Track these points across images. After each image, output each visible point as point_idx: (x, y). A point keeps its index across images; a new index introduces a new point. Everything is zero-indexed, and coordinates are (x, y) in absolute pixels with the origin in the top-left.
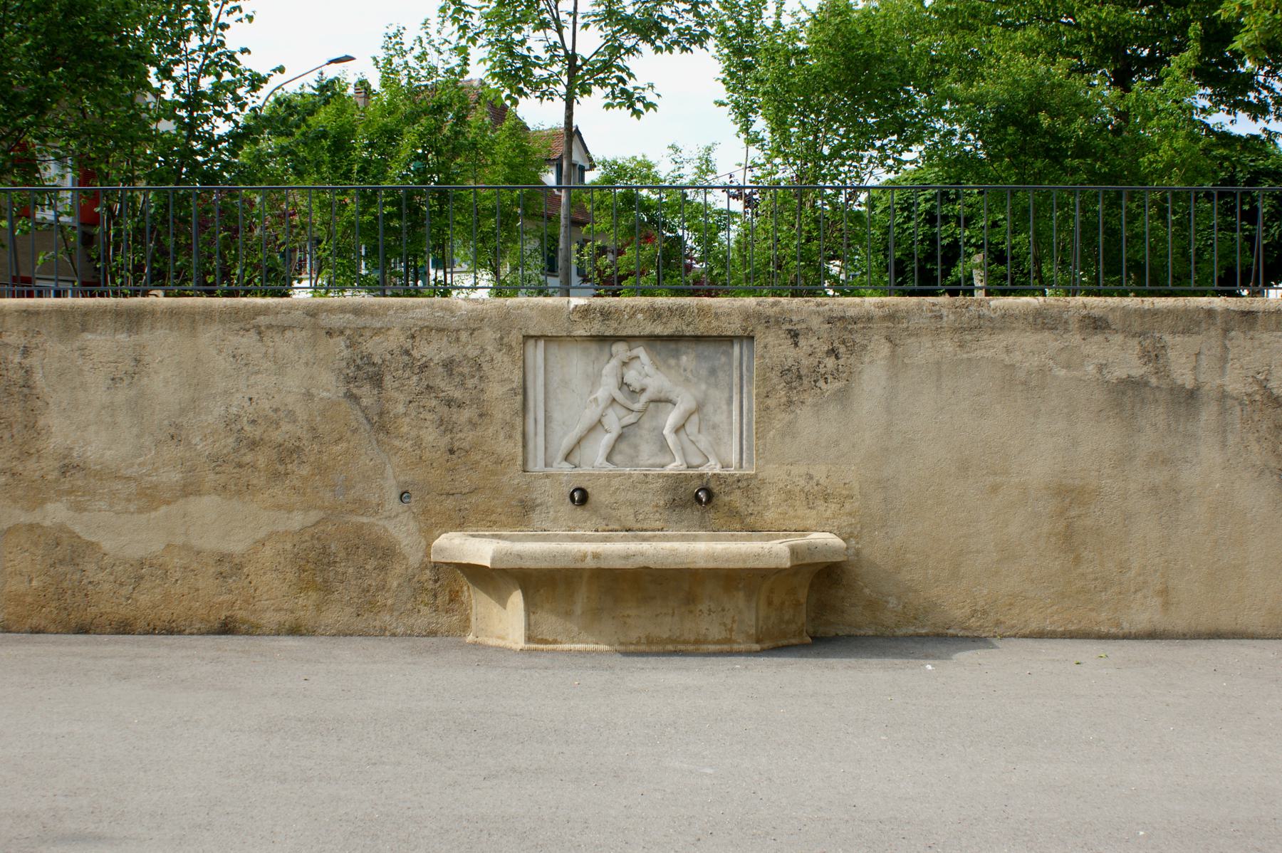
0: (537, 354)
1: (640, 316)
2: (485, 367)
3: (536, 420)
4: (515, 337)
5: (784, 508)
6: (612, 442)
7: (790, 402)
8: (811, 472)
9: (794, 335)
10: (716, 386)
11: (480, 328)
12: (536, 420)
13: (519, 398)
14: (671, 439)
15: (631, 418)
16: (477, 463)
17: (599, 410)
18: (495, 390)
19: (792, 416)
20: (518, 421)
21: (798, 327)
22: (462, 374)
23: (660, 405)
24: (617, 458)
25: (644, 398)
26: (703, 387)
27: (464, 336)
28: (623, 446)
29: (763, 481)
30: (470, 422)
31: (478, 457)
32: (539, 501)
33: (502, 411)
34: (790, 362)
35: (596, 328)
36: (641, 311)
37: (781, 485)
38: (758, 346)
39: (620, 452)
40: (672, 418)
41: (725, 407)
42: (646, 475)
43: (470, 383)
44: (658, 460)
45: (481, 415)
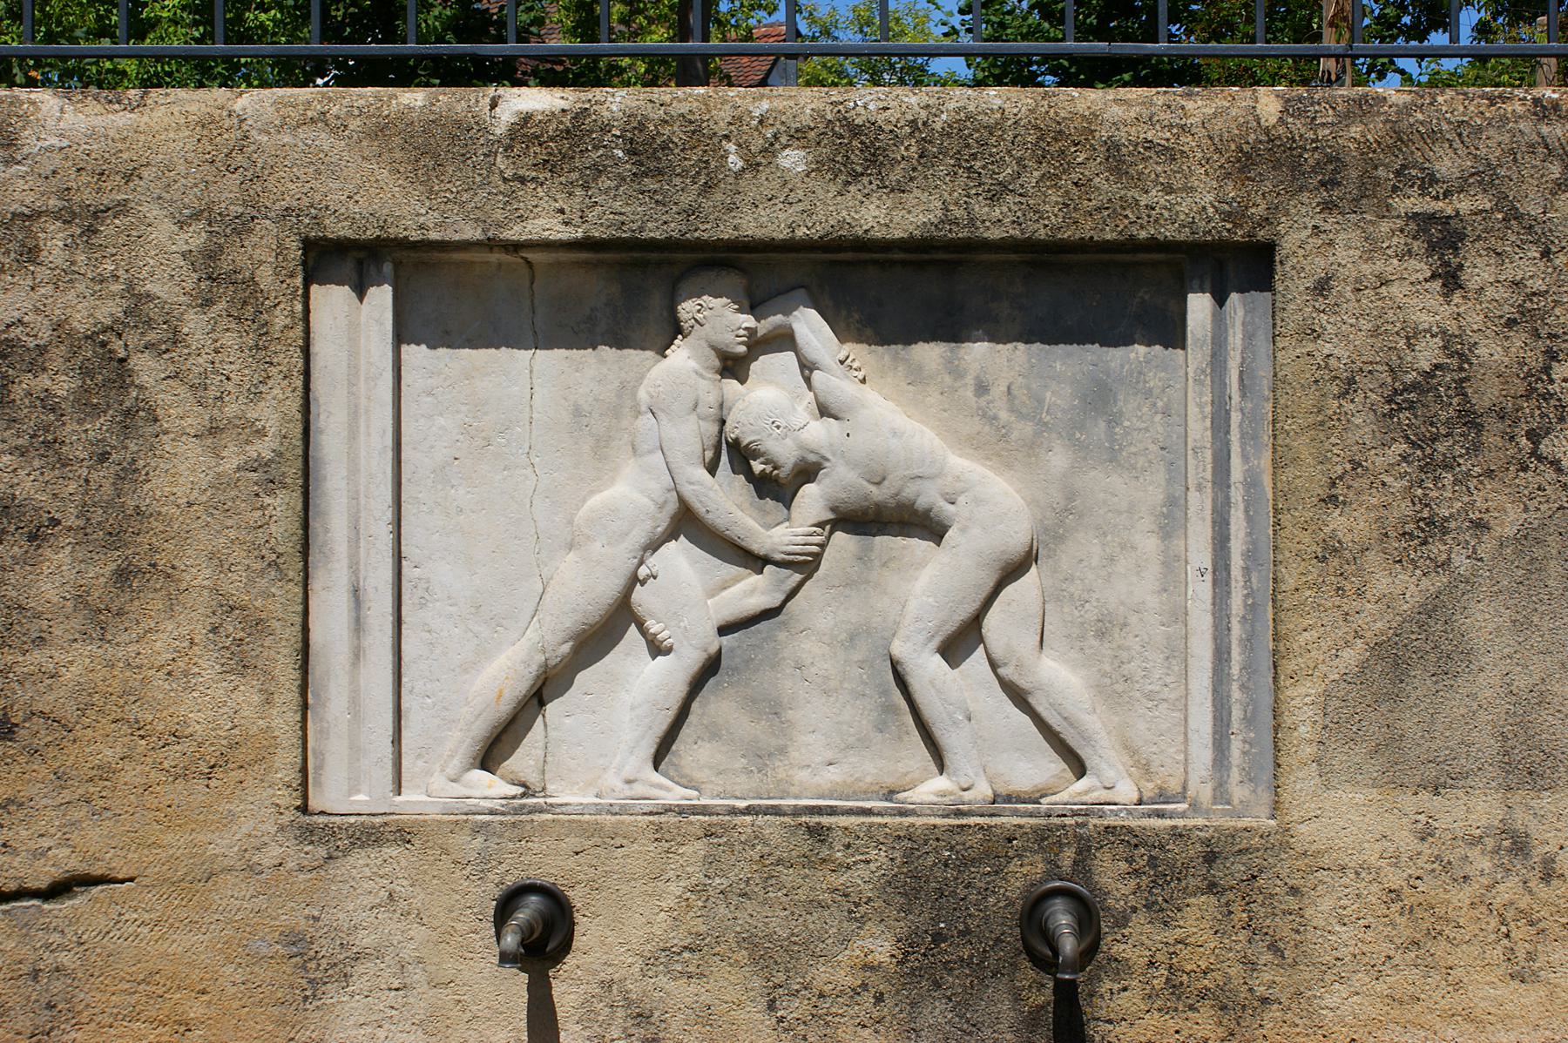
1: (792, 159)
2: (146, 368)
4: (265, 256)
5: (1403, 978)
7: (1432, 527)
8: (1521, 819)
9: (1442, 240)
10: (1113, 456)
11: (122, 208)
13: (283, 504)
14: (928, 668)
15: (752, 591)
16: (105, 773)
17: (620, 560)
18: (182, 470)
19: (1441, 580)
20: (279, 600)
21: (1464, 205)
22: (46, 402)
23: (883, 543)
24: (692, 751)
25: (812, 500)
26: (1058, 459)
27: (54, 242)
28: (716, 705)
29: (1314, 862)
30: (81, 600)
31: (109, 754)
32: (365, 940)
33: (208, 559)
34: (1427, 354)
35: (616, 211)
36: (799, 136)
37: (1395, 879)
38: (1293, 281)
39: (714, 733)
40: (922, 586)
41: (1150, 544)
43: (79, 435)
45: (123, 576)
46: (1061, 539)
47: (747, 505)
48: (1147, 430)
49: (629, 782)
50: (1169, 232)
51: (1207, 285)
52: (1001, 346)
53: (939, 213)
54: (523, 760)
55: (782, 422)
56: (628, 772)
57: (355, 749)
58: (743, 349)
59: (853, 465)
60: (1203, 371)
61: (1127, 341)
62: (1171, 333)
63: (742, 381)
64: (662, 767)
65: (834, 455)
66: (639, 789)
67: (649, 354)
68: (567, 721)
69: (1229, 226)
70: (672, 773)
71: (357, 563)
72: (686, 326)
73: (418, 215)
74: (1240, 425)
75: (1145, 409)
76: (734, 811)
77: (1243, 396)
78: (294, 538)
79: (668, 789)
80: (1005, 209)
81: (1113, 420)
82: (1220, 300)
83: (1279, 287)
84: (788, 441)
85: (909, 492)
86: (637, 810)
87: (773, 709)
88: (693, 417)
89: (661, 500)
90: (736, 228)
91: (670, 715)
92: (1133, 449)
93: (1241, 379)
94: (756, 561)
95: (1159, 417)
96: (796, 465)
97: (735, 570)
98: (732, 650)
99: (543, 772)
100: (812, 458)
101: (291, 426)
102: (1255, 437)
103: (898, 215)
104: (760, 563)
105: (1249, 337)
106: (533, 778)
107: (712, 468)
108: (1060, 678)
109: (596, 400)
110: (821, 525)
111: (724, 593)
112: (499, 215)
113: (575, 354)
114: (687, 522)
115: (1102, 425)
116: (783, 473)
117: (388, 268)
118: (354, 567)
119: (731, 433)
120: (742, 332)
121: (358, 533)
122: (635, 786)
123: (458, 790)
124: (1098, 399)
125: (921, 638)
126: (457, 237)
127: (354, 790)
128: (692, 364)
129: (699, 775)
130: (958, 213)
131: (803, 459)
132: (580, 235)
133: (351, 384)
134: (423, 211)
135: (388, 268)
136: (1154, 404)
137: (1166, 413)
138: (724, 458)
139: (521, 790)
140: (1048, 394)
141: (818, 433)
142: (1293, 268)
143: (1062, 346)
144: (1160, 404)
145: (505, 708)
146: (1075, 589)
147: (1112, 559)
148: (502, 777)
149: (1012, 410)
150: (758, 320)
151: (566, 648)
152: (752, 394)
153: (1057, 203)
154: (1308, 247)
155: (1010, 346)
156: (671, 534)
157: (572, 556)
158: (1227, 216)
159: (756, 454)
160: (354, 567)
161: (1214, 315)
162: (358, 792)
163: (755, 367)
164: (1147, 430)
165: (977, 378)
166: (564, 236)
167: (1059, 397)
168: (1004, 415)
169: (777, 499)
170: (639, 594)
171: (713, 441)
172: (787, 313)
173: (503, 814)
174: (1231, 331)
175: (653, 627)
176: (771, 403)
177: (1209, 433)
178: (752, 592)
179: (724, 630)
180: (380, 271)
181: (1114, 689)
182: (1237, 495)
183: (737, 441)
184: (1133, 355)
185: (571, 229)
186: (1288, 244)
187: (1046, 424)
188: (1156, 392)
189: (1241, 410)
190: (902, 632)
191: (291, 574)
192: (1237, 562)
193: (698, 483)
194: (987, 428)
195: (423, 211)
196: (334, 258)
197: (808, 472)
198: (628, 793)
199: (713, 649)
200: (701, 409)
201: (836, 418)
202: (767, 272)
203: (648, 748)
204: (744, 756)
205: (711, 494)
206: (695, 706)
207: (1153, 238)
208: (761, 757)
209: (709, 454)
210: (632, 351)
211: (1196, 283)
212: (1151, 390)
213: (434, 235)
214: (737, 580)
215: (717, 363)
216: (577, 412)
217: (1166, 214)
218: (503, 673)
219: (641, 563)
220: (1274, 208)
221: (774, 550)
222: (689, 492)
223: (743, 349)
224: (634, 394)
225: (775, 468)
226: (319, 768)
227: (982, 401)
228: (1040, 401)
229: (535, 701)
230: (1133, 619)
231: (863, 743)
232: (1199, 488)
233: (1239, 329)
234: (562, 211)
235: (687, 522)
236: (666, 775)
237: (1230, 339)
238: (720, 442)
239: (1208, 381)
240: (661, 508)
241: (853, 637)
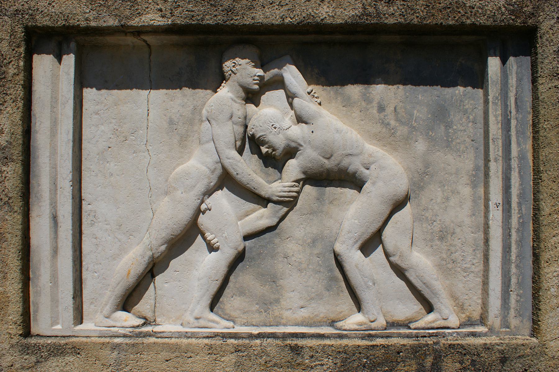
0: (54, 75)
3: (55, 218)
6: (223, 270)
10: (448, 144)
12: (55, 218)
14: (354, 258)
15: (261, 217)
23: (330, 190)
24: (230, 301)
25: (293, 168)
26: (421, 146)
28: (243, 277)
39: (242, 292)
40: (353, 212)
41: (466, 191)
42: (296, 350)
44: (323, 310)
46: (421, 188)
47: (258, 171)
48: (465, 131)
49: (197, 319)
50: (482, 21)
51: (498, 53)
52: (390, 87)
53: (361, 10)
54: (144, 305)
55: (277, 125)
56: (196, 313)
57: (55, 301)
58: (256, 87)
59: (315, 148)
60: (497, 98)
61: (453, 84)
62: (478, 80)
63: (257, 106)
64: (215, 309)
65: (305, 143)
66: (202, 323)
67: (209, 91)
68: (166, 285)
69: (513, 17)
70: (220, 313)
71: (56, 202)
72: (227, 74)
73: (85, 13)
74: (516, 127)
75: (464, 120)
76: (251, 336)
77: (517, 111)
78: (18, 189)
79: (217, 323)
80: (396, 8)
81: (448, 126)
82: (504, 61)
83: (540, 50)
84: (281, 136)
85: (345, 162)
86: (200, 335)
87: (272, 279)
88: (230, 123)
89: (213, 168)
90: (253, 18)
91: (219, 283)
92: (458, 141)
93: (516, 103)
94: (264, 201)
95: (470, 124)
96: (284, 148)
97: (252, 206)
98: (251, 248)
99: (154, 312)
100: (293, 145)
101: (16, 127)
102: (523, 133)
103: (339, 11)
104: (265, 202)
105: (519, 80)
106: (149, 315)
107: (241, 151)
108: (422, 262)
109: (181, 116)
110: (297, 181)
111: (247, 218)
112: (127, 13)
113: (170, 91)
114: (227, 180)
115: (443, 128)
116: (278, 153)
117: (73, 45)
118: (54, 204)
119: (250, 132)
120: (256, 78)
121: (56, 186)
122: (200, 321)
123: (110, 322)
124: (440, 114)
125: (351, 242)
126: (105, 25)
127: (55, 322)
128: (230, 95)
129: (234, 314)
130: (371, 10)
131: (288, 146)
132: (170, 22)
133: (53, 107)
134: (88, 11)
135: (73, 45)
136: (468, 117)
137: (474, 122)
138: (247, 146)
139: (142, 321)
140: (415, 112)
141: (297, 132)
142: (547, 40)
143: (422, 87)
144: (471, 117)
145: (131, 280)
146: (429, 214)
147: (447, 199)
148: (134, 314)
149: (397, 120)
150: (265, 72)
151: (163, 248)
152: (262, 111)
153: (423, 5)
154: (555, 29)
155: (395, 86)
156: (219, 187)
157: (167, 199)
158: (512, 12)
159: (263, 143)
160: (54, 204)
161: (501, 69)
162: (58, 323)
163: (263, 98)
164: (465, 131)
165: (379, 103)
166: (161, 23)
167: (421, 113)
168: (393, 123)
169: (275, 167)
170: (202, 219)
172: (280, 68)
173: (130, 337)
174: (510, 77)
175: (209, 236)
176: (271, 116)
177: (500, 131)
178: (262, 217)
179: (247, 238)
180: (68, 47)
181: (447, 267)
182: (514, 164)
183: (253, 136)
184: (457, 92)
185: (165, 20)
186: (545, 26)
187: (414, 127)
188: (469, 111)
189: (516, 118)
190: (341, 239)
191: (16, 208)
192: (515, 200)
193: (233, 158)
194: (384, 130)
195: (88, 11)
196: (42, 38)
197: (291, 152)
198: (197, 325)
199: (241, 248)
200: (235, 119)
201: (306, 123)
202: (271, 44)
203: (207, 301)
204: (257, 304)
205: (239, 164)
206: (232, 278)
207: (473, 24)
208: (266, 304)
209: (239, 143)
210: (200, 90)
211: (492, 51)
212: (466, 110)
213: (93, 24)
214: (254, 211)
215: (243, 94)
216: (171, 122)
217: (480, 11)
218: (130, 261)
219: (202, 202)
220: (536, 8)
221: (273, 195)
222: (227, 163)
223: (256, 87)
224: (200, 113)
225: (274, 150)
226: (36, 311)
227: (382, 116)
228: (411, 115)
229: (150, 275)
230: (458, 230)
231: (319, 297)
232: (496, 160)
233: (514, 75)
234: (161, 10)
235: (227, 180)
236: (217, 314)
237: (510, 81)
239: (499, 104)
240: (213, 172)
241: (314, 241)
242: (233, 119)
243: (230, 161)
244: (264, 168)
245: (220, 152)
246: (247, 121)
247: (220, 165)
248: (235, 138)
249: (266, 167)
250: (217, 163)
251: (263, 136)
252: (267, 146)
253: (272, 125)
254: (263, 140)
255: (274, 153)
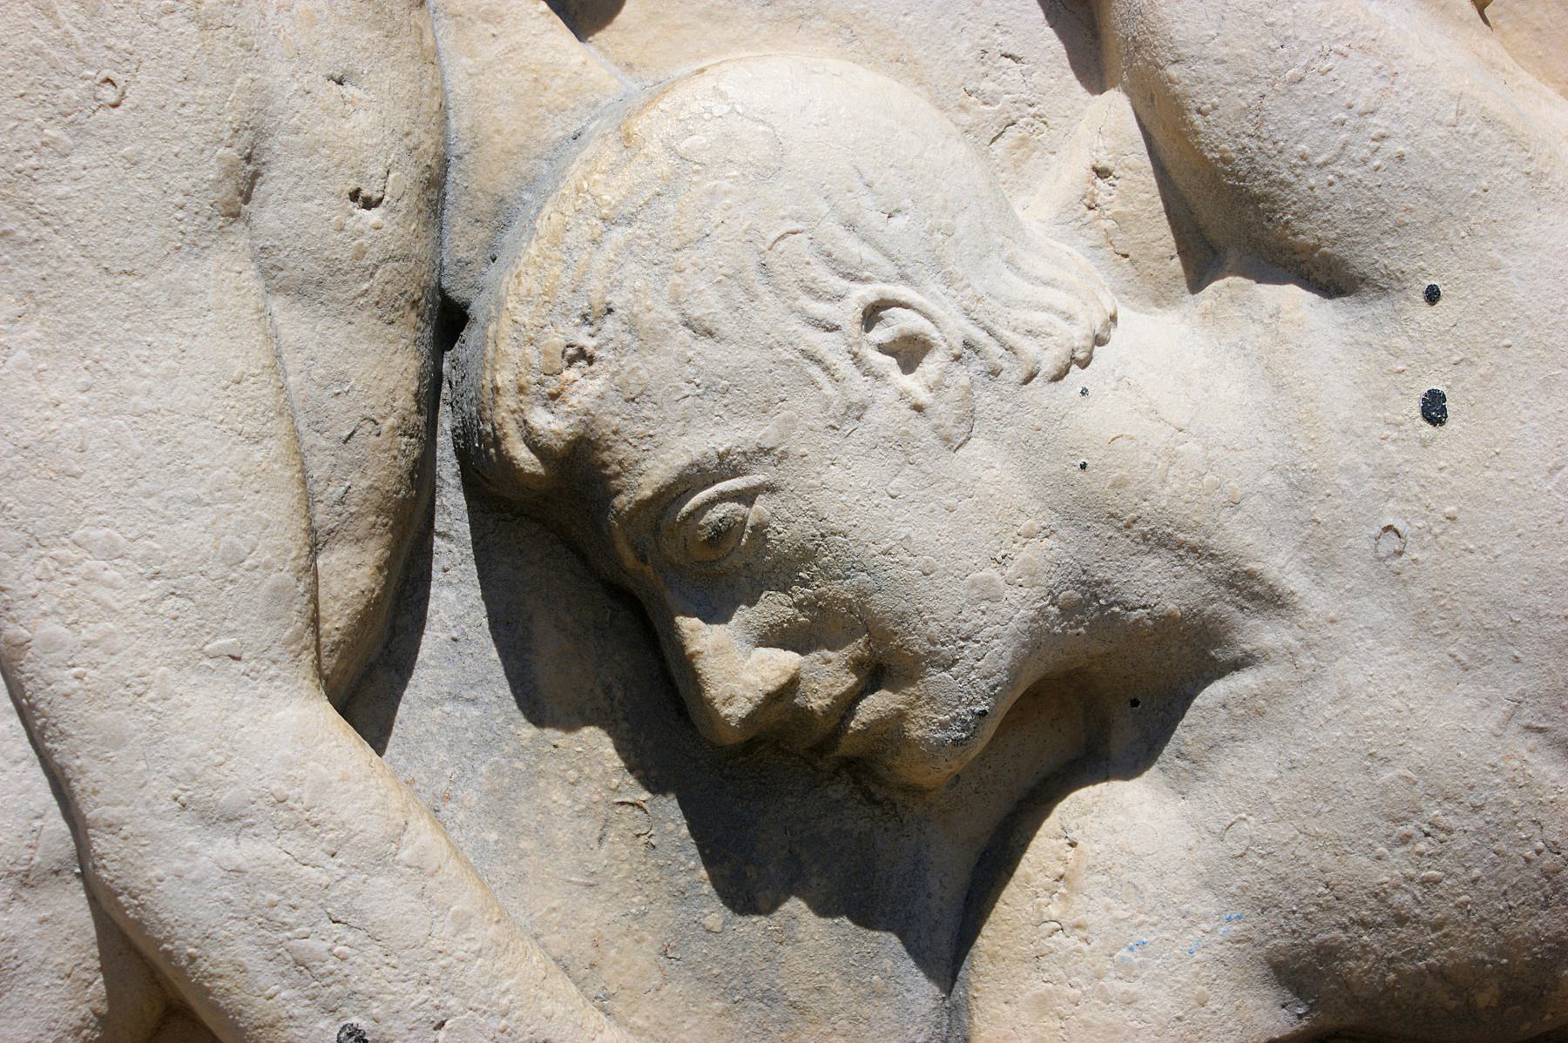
47: (634, 960)
55: (937, 311)
59: (1471, 635)
65: (1323, 562)
84: (986, 464)
88: (226, 274)
96: (1036, 641)
100: (1156, 586)
107: (367, 681)
116: (941, 710)
131: (1085, 602)
138: (455, 599)
141: (1200, 395)
152: (693, 97)
159: (727, 568)
169: (860, 899)
171: (376, 470)
183: (581, 467)
193: (287, 813)
200: (295, 209)
201: (1331, 279)
205: (387, 899)
209: (351, 574)
222: (193, 887)
238: (422, 474)
242: (268, 216)
243: (228, 849)
244: (715, 914)
245: (89, 772)
246: (462, 240)
247: (73, 906)
248: (309, 500)
249: (744, 891)
250: (27, 881)
251: (726, 466)
252: (774, 607)
253: (872, 315)
254: (724, 534)
255: (877, 704)
